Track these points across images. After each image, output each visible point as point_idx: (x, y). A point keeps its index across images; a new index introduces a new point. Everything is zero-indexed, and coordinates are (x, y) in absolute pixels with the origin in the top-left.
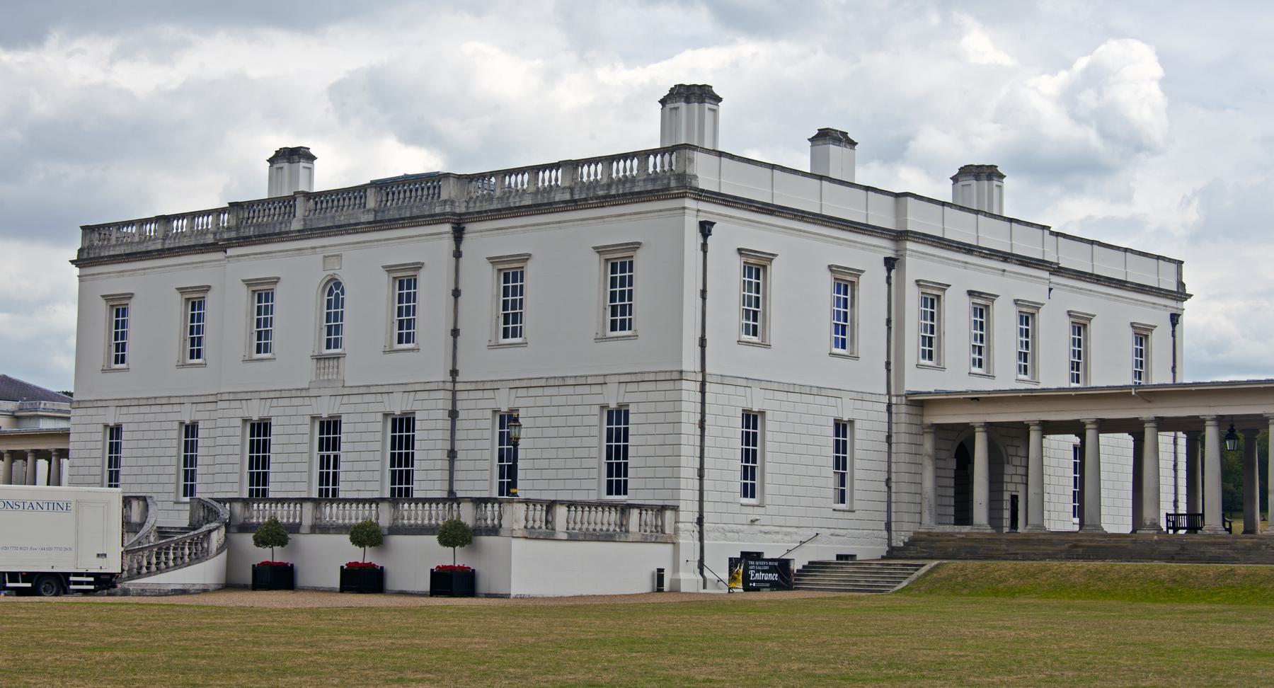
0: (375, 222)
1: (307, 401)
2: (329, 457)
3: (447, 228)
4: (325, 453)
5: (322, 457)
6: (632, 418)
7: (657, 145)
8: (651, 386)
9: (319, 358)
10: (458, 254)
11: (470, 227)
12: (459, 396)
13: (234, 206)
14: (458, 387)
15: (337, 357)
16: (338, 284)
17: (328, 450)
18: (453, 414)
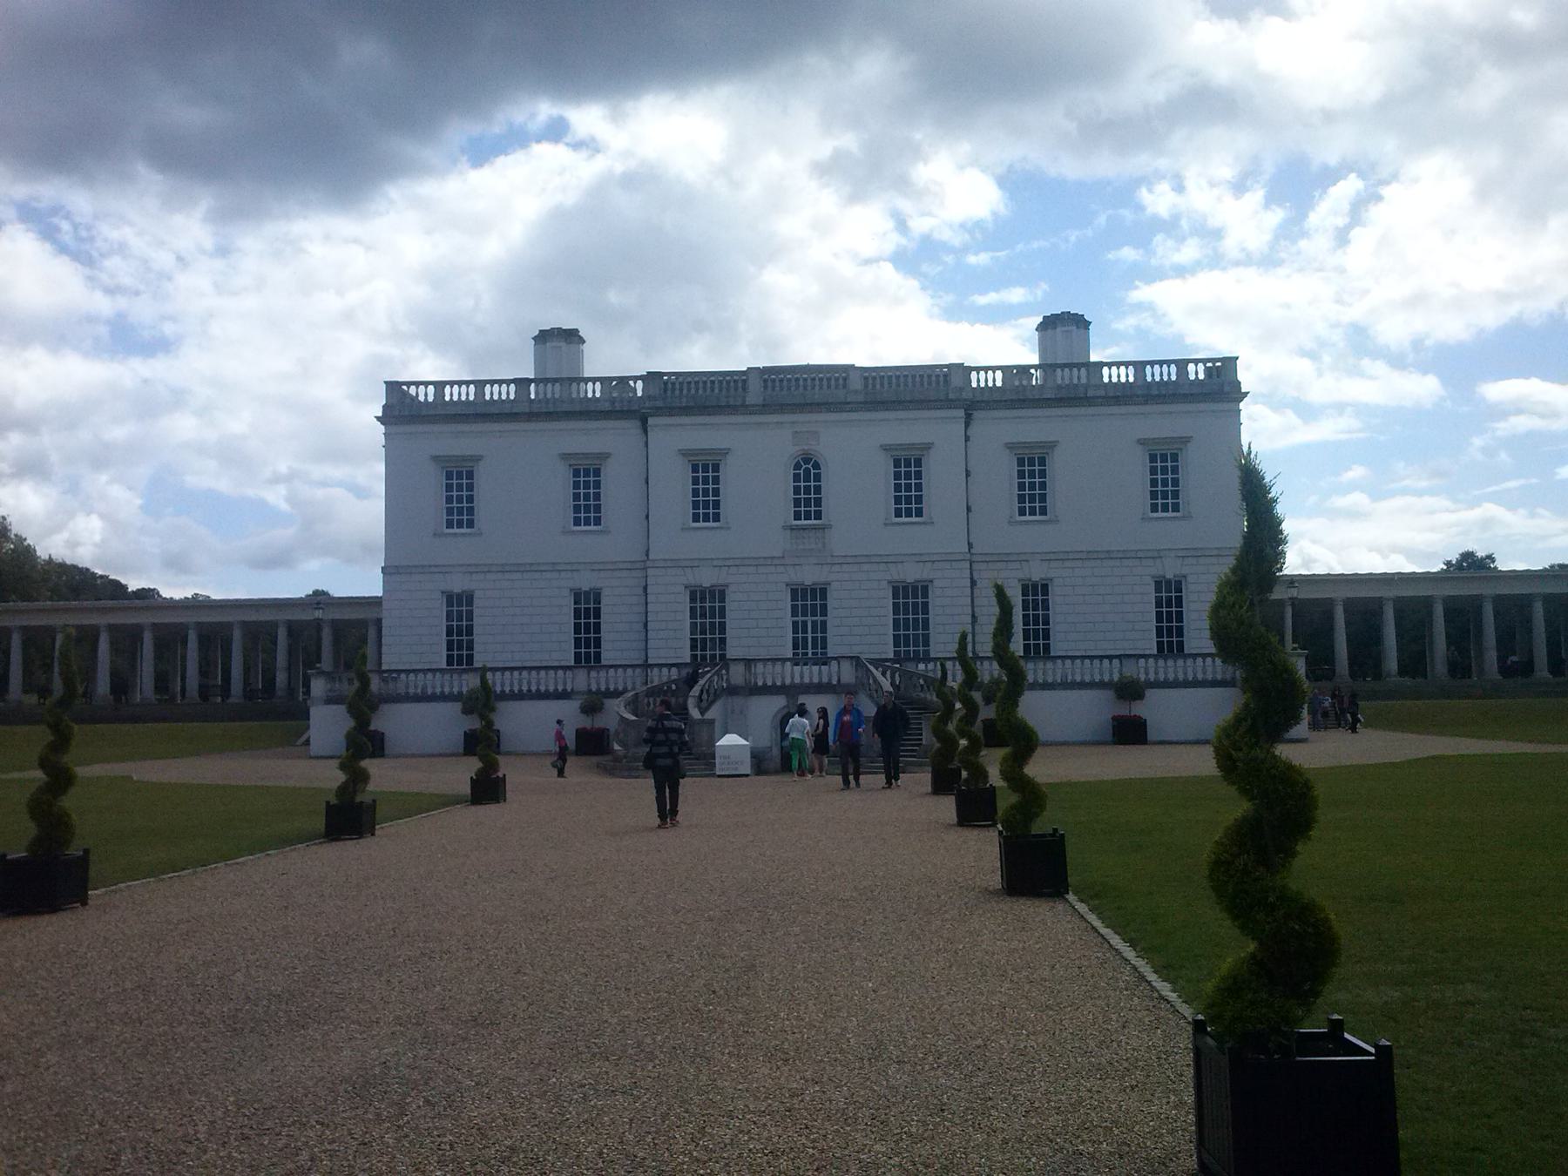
0: (865, 403)
1: (781, 569)
2: (805, 623)
3: (961, 413)
4: (800, 619)
5: (795, 624)
6: (476, 602)
7: (1037, 362)
8: (1214, 560)
9: (792, 528)
10: (967, 439)
11: (976, 414)
12: (975, 566)
13: (651, 378)
14: (975, 558)
15: (823, 528)
16: (807, 461)
17: (804, 614)
18: (973, 583)
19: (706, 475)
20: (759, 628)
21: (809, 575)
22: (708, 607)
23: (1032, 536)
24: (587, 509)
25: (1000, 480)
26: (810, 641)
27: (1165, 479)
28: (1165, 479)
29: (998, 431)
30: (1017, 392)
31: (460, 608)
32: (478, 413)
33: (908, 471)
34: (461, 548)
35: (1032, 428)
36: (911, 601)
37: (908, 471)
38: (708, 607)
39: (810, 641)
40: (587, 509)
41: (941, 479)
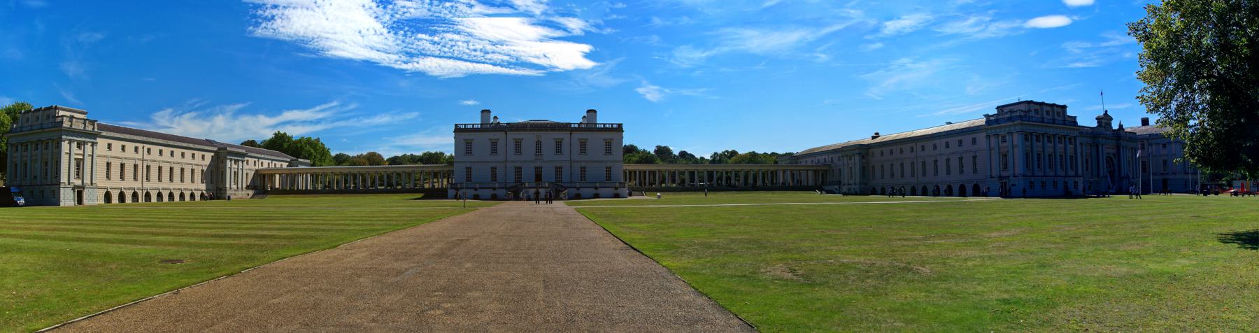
19: (518, 144)
20: (528, 174)
21: (538, 164)
22: (518, 170)
23: (584, 157)
24: (494, 150)
25: (577, 148)
26: (538, 177)
27: (608, 149)
28: (608, 149)
29: (577, 135)
30: (580, 129)
31: (469, 170)
32: (474, 130)
33: (559, 144)
34: (469, 158)
35: (584, 135)
36: (559, 170)
37: (559, 144)
38: (518, 170)
39: (538, 177)
40: (494, 150)
41: (565, 147)
